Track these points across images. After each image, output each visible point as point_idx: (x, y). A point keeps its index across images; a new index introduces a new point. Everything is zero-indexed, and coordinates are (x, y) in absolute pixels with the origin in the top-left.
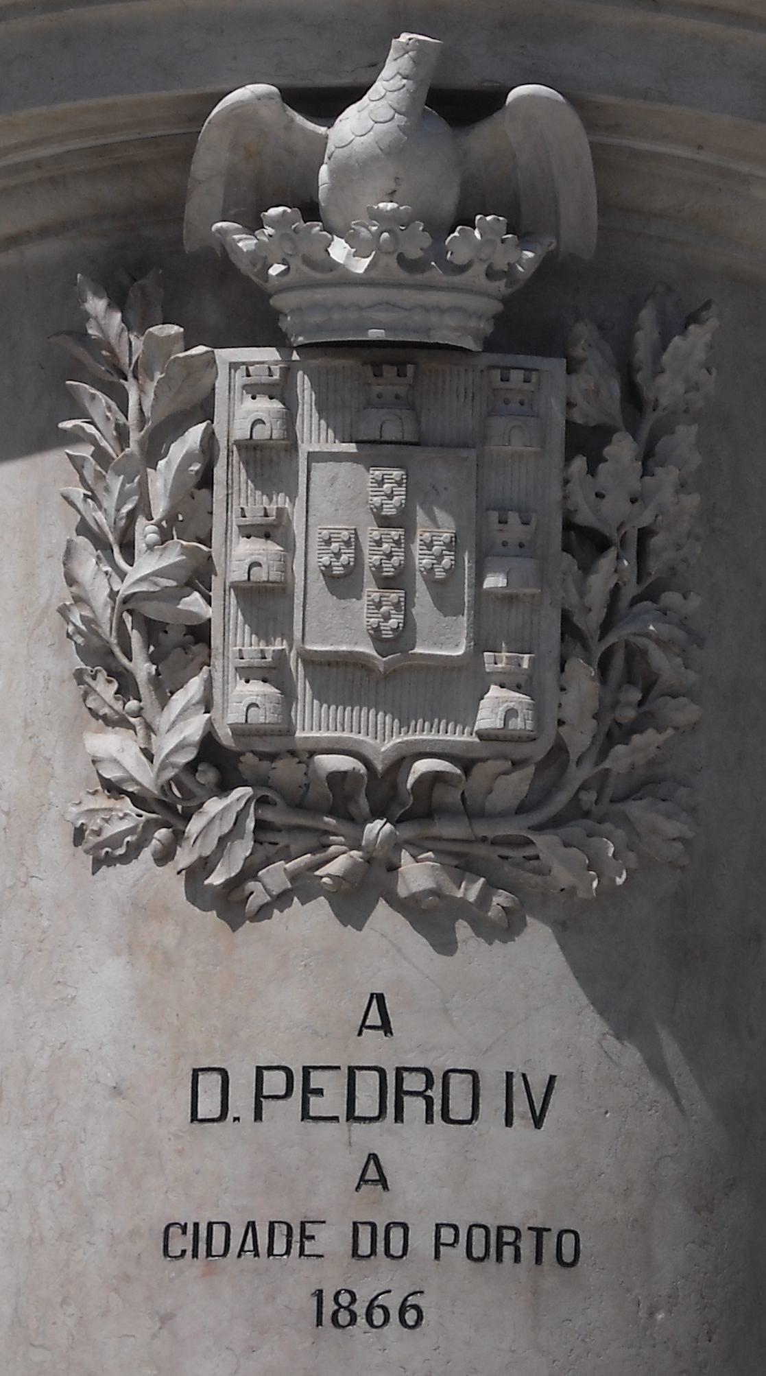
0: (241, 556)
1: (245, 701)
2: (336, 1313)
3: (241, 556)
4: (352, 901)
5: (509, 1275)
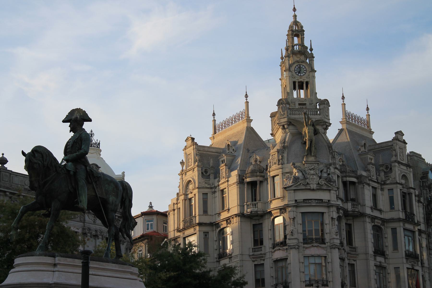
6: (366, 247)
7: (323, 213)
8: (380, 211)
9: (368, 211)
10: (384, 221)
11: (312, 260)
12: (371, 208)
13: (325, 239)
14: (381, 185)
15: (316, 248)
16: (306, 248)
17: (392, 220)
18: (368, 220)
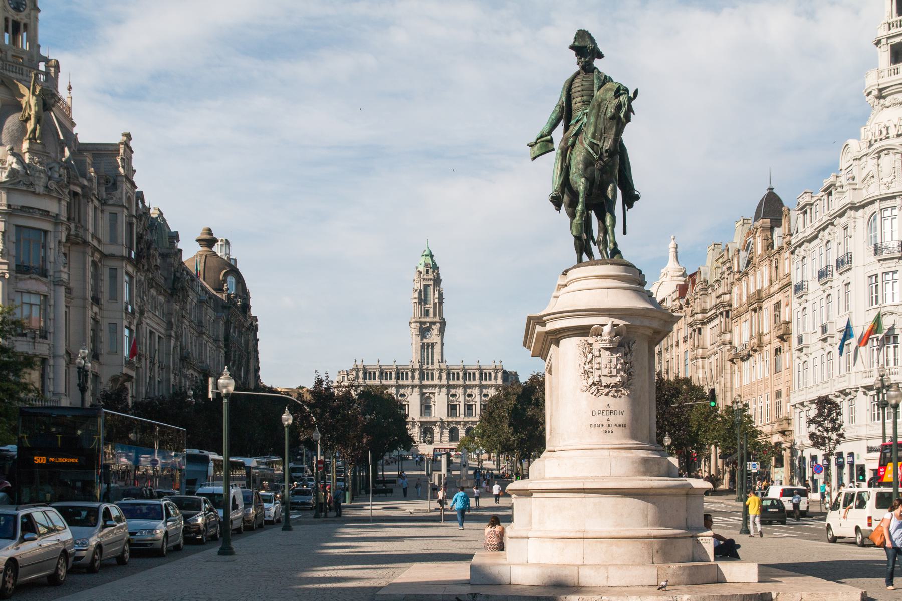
0: (596, 366)
1: (597, 379)
2: (606, 432)
3: (596, 366)
4: (607, 394)
5: (620, 428)
6: (84, 289)
7: (46, 232)
8: (99, 241)
9: (89, 239)
10: (104, 256)
11: (26, 298)
12: (92, 235)
13: (46, 270)
14: (103, 204)
15: (34, 281)
16: (21, 280)
17: (112, 257)
18: (89, 251)
